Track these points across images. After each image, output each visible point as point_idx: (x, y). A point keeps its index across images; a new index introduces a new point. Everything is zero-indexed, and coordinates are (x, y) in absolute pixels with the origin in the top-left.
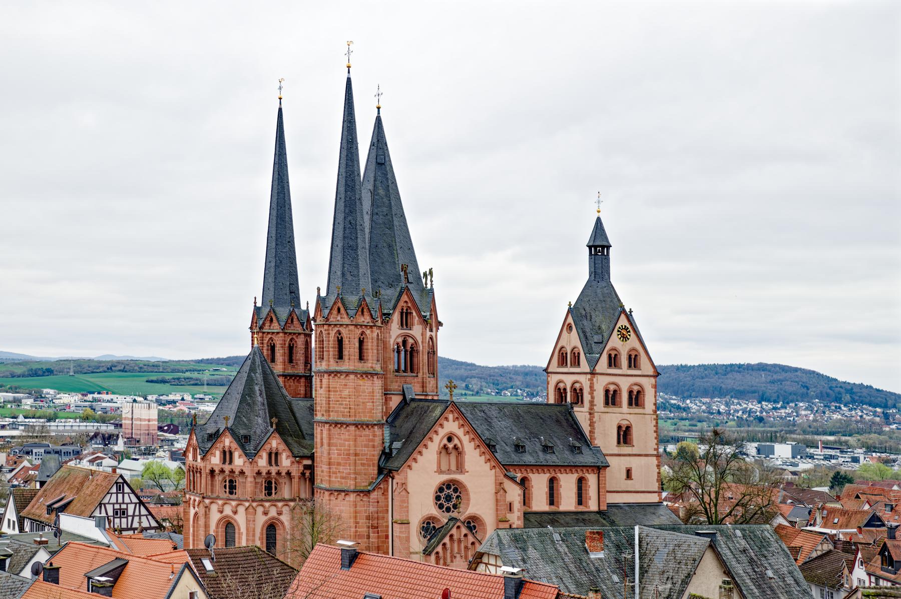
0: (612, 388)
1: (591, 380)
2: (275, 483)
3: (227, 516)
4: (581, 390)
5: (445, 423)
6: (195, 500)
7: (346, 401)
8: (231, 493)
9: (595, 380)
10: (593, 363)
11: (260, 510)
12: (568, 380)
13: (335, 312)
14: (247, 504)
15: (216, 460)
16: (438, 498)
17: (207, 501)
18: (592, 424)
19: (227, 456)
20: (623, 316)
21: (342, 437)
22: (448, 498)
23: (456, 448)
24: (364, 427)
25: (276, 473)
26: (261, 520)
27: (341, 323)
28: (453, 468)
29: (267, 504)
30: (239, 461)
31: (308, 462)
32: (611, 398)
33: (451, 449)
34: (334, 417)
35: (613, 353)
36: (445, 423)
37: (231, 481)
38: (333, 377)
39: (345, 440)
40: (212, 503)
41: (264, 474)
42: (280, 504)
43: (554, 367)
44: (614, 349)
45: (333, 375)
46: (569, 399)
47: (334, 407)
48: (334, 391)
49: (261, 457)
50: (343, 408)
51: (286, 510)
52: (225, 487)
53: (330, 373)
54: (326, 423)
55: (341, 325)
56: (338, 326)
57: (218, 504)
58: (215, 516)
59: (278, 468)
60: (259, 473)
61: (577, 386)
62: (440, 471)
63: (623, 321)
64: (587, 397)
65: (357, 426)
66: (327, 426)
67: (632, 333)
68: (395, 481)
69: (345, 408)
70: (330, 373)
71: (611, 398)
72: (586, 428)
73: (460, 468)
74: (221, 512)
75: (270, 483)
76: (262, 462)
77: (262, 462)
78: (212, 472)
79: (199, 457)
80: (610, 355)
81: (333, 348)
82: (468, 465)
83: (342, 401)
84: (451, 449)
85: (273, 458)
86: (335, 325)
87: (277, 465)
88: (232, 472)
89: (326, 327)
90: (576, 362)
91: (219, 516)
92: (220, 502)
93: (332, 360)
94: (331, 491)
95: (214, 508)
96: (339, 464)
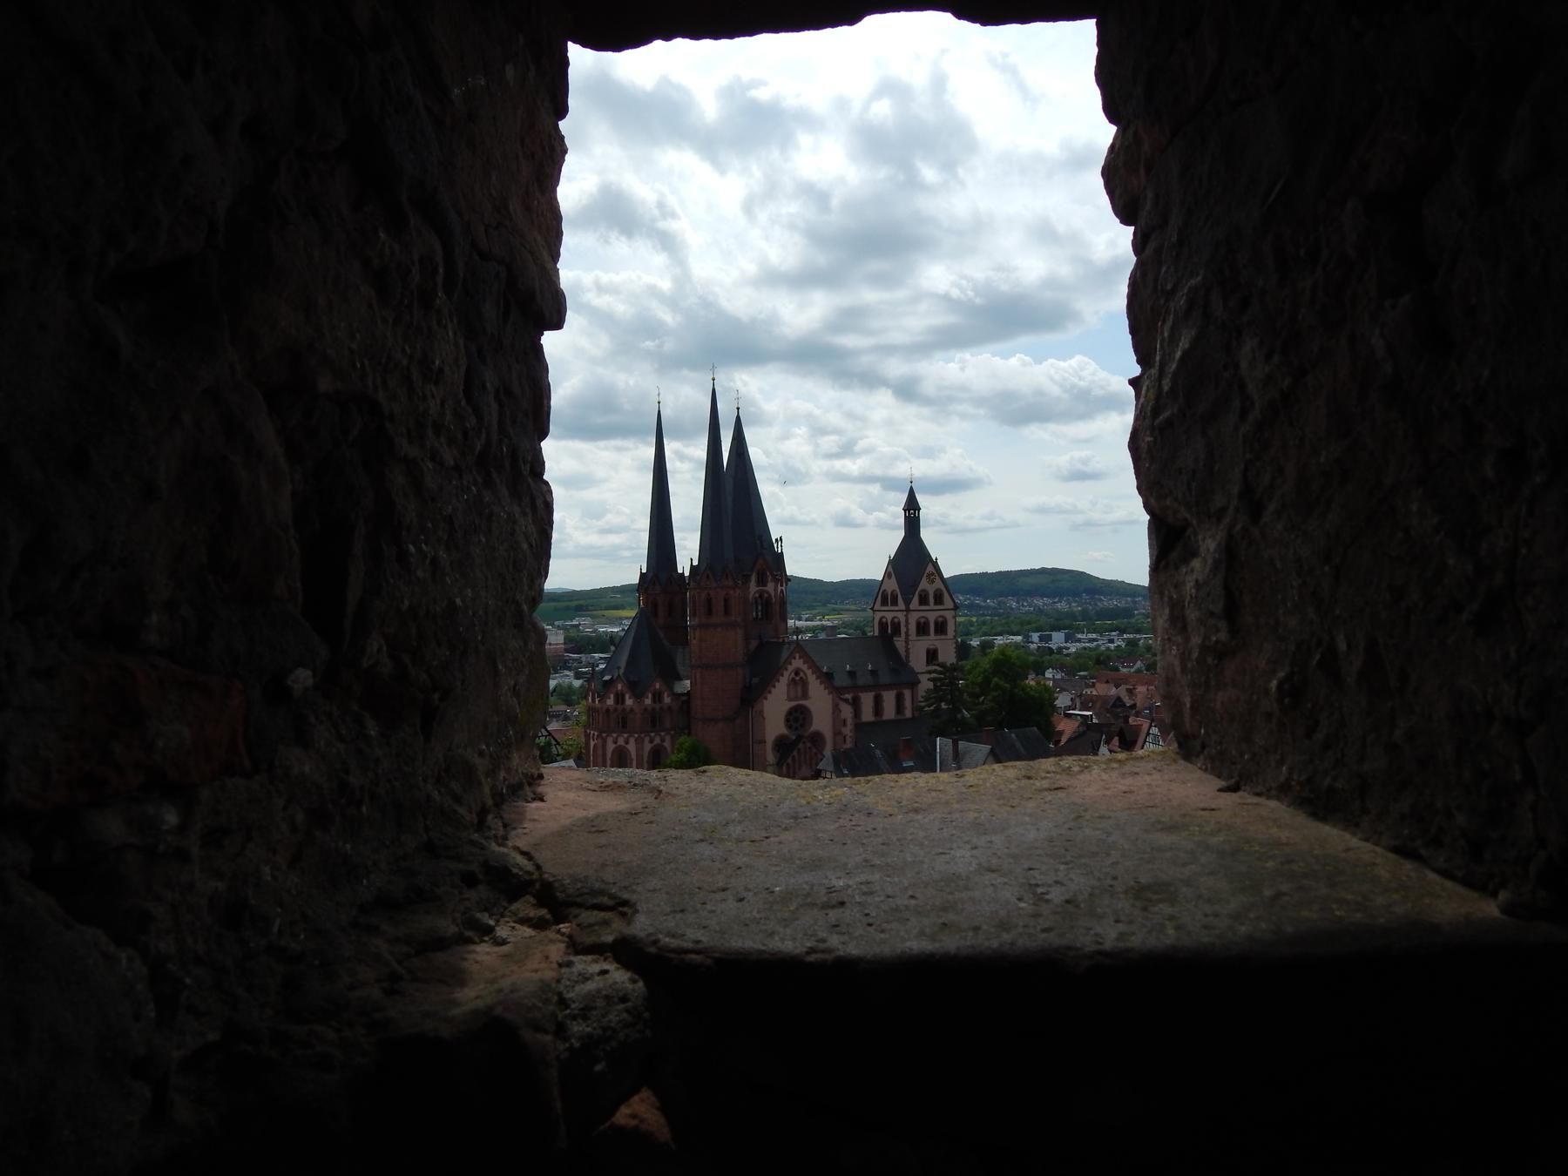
0: (922, 620)
1: (906, 616)
3: (620, 746)
4: (899, 623)
5: (793, 661)
6: (594, 734)
8: (623, 727)
9: (909, 616)
10: (908, 602)
11: (647, 740)
12: (889, 616)
14: (636, 735)
15: (610, 701)
16: (787, 720)
17: (604, 735)
18: (907, 650)
19: (620, 699)
20: (930, 564)
22: (796, 720)
23: (801, 678)
26: (648, 747)
28: (800, 694)
29: (652, 734)
30: (629, 702)
31: (684, 698)
32: (922, 629)
33: (799, 683)
35: (923, 594)
36: (793, 661)
37: (623, 718)
40: (607, 736)
42: (663, 734)
43: (878, 606)
44: (924, 590)
46: (889, 631)
49: (647, 698)
51: (668, 738)
52: (619, 723)
58: (611, 747)
60: (646, 710)
61: (896, 620)
62: (790, 699)
63: (930, 568)
64: (903, 630)
67: (937, 577)
68: (754, 710)
71: (922, 629)
72: (903, 654)
73: (805, 695)
74: (616, 743)
76: (648, 701)
77: (648, 701)
78: (608, 710)
79: (597, 702)
80: (920, 596)
82: (811, 693)
84: (799, 683)
85: (658, 697)
88: (624, 710)
90: (895, 602)
91: (614, 746)
92: (615, 735)
95: (610, 740)
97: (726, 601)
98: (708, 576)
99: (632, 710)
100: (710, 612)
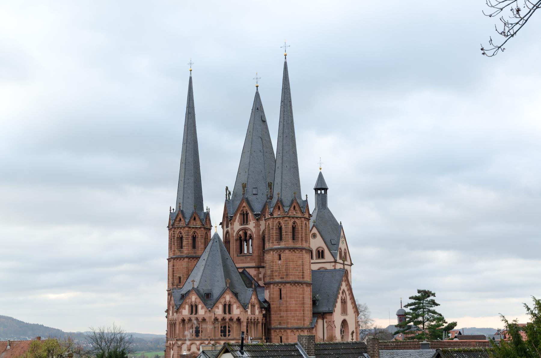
2: (229, 327)
7: (300, 268)
13: (292, 208)
21: (298, 292)
24: (293, 284)
25: (229, 320)
27: (297, 216)
34: (291, 279)
38: (292, 252)
39: (300, 294)
41: (220, 320)
45: (276, 251)
47: (292, 272)
48: (292, 261)
50: (298, 272)
53: (290, 249)
54: (288, 283)
55: (297, 218)
56: (295, 218)
57: (196, 344)
59: (230, 316)
65: (291, 284)
66: (288, 285)
69: (300, 273)
70: (290, 249)
75: (225, 327)
81: (290, 232)
83: (297, 268)
86: (293, 218)
87: (230, 313)
89: (271, 220)
93: (290, 241)
94: (292, 329)
96: (296, 310)
97: (294, 228)
98: (294, 207)
99: (204, 320)
100: (293, 239)
